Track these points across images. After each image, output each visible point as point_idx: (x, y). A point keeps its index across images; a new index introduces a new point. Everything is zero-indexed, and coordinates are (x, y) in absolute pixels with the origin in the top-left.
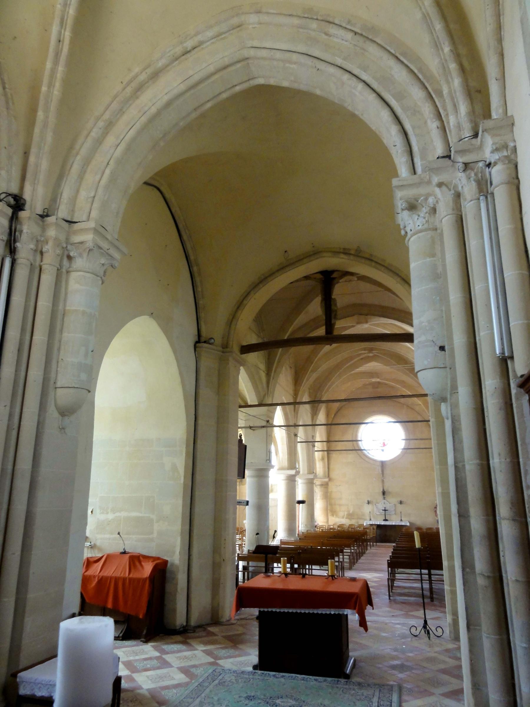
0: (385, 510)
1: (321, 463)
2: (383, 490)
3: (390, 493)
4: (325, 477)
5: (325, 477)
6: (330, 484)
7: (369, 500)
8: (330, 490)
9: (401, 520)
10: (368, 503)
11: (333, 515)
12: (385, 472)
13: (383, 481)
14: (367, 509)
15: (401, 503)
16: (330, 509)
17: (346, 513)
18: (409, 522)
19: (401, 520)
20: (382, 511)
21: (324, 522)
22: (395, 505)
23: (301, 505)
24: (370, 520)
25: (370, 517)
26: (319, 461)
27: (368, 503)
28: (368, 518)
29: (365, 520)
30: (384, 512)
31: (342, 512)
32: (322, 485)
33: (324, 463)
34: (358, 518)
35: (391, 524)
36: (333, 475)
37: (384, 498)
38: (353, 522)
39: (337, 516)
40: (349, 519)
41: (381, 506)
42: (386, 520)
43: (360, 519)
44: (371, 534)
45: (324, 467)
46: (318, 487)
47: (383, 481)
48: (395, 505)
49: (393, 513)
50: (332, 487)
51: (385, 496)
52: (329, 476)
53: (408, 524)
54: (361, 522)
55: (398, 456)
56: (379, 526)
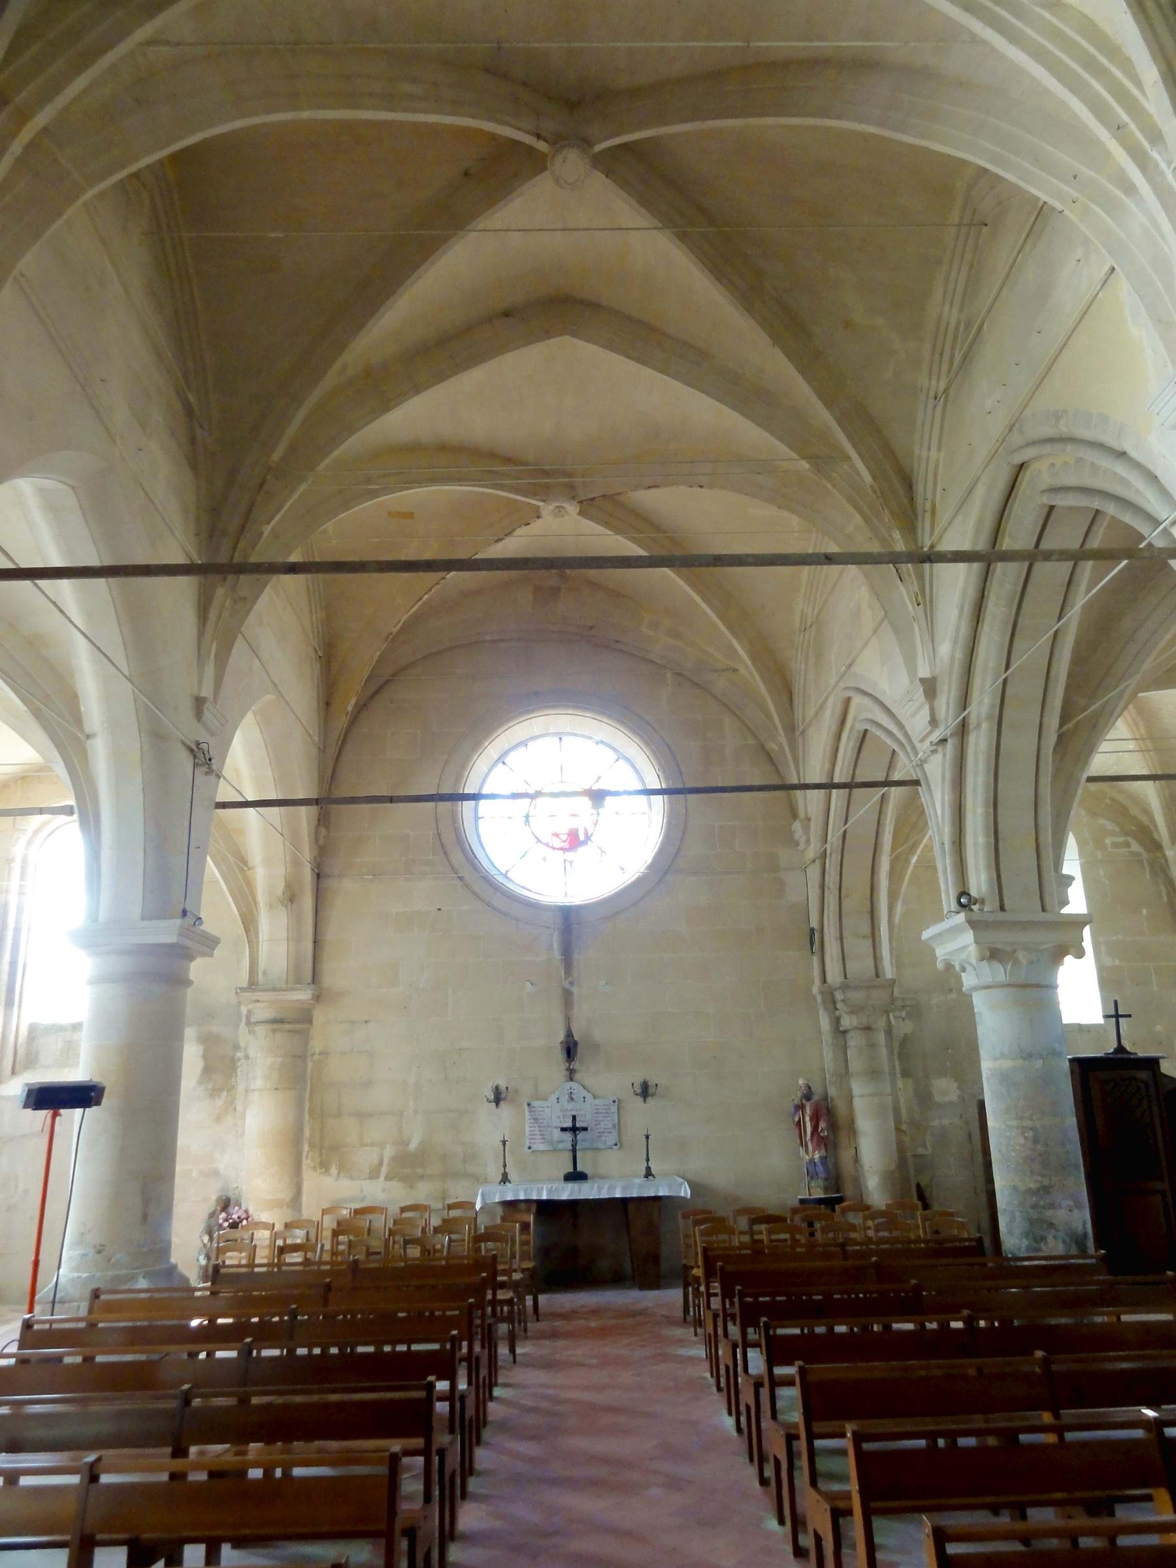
0: (574, 1129)
1: (282, 917)
2: (569, 1034)
3: (595, 1047)
4: (298, 980)
5: (298, 980)
6: (319, 1016)
7: (503, 1086)
8: (316, 1045)
9: (648, 1173)
10: (498, 1098)
11: (324, 1166)
12: (576, 956)
13: (567, 998)
14: (490, 1128)
15: (645, 1091)
16: (310, 1135)
17: (389, 1152)
18: (692, 1185)
19: (648, 1173)
20: (557, 1134)
21: (276, 1204)
22: (618, 1102)
23: (72, 1116)
24: (505, 1179)
25: (504, 1167)
27: (498, 1098)
29: (479, 1180)
30: (568, 1136)
31: (373, 1145)
32: (281, 1021)
33: (298, 918)
35: (604, 1195)
37: (571, 1074)
38: (422, 1193)
39: (345, 1169)
40: (403, 1179)
41: (556, 1114)
42: (576, 1176)
44: (518, 1257)
45: (295, 936)
46: (261, 1030)
47: (567, 998)
48: (618, 1102)
49: (612, 1139)
50: (331, 1033)
51: (576, 1065)
52: (315, 977)
53: (685, 1192)
54: (458, 1191)
56: (547, 1209)
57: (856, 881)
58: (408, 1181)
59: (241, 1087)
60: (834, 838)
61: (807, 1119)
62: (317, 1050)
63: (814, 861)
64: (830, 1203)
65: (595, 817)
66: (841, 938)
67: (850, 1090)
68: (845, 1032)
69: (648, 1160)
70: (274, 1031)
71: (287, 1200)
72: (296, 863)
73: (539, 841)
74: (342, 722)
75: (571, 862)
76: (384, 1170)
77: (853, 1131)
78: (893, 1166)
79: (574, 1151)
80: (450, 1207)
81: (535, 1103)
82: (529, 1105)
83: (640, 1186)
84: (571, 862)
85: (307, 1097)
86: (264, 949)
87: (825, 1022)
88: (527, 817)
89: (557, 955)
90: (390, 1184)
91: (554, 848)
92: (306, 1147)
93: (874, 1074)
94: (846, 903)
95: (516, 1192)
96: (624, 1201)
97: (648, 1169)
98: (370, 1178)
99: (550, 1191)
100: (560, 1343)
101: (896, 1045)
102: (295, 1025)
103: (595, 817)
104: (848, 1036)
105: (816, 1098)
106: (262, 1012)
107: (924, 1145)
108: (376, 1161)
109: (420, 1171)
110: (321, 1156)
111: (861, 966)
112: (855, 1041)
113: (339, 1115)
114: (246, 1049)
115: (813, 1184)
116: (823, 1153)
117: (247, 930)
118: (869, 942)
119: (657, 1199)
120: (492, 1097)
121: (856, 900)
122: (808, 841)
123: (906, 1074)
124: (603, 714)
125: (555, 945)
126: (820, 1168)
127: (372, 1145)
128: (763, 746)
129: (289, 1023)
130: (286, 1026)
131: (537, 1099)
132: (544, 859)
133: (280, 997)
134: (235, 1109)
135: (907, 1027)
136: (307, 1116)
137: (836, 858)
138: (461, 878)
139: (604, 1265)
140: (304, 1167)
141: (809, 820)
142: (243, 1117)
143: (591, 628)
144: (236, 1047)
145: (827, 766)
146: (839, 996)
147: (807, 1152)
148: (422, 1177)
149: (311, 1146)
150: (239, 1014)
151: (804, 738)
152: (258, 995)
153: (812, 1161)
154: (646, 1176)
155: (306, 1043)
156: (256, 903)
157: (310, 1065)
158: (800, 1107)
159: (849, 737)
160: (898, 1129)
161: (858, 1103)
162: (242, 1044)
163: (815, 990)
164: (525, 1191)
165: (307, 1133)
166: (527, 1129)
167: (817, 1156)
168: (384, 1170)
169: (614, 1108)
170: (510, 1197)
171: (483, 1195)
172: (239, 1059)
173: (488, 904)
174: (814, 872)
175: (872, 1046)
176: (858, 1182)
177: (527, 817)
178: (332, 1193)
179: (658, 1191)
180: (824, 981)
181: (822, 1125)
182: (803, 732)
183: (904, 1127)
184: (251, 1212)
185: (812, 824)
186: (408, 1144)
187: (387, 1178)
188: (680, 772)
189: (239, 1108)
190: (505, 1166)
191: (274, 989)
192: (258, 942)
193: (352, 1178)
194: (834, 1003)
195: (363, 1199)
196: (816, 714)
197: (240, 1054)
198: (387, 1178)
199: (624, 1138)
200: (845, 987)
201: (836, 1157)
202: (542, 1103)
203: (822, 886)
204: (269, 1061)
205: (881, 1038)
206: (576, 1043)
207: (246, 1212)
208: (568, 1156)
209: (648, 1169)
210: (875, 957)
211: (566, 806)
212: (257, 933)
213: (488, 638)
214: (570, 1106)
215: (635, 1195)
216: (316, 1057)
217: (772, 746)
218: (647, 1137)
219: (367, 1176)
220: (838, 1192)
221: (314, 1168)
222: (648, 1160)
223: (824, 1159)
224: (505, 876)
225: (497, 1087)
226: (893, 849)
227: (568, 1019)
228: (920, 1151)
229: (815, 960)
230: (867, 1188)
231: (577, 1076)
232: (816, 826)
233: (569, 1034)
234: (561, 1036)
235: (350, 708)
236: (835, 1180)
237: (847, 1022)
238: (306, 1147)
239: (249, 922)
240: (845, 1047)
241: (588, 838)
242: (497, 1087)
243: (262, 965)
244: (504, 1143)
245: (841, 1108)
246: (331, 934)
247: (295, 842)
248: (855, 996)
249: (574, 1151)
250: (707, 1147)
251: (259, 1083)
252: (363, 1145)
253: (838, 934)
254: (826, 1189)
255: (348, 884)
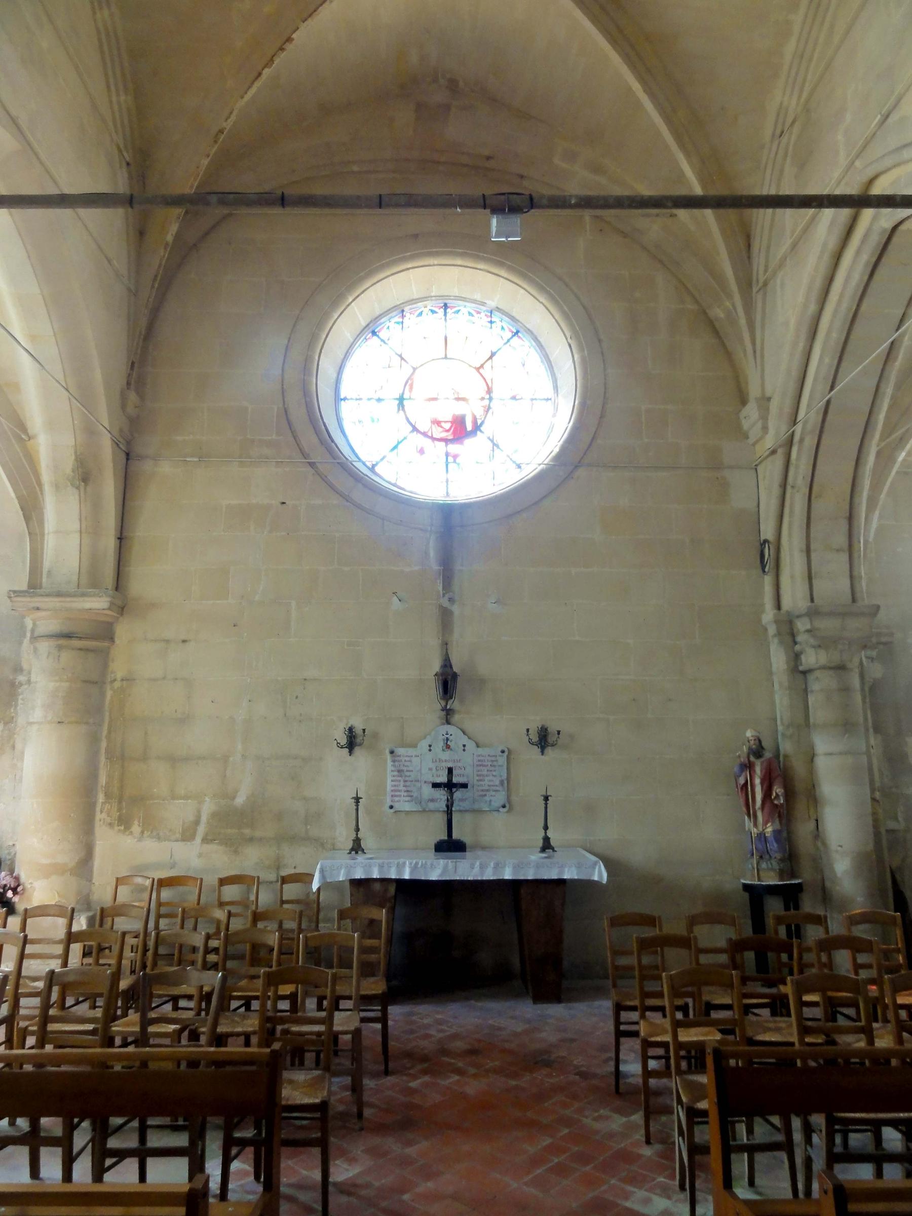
0: (450, 786)
2: (447, 664)
3: (481, 683)
6: (122, 631)
7: (359, 726)
8: (118, 668)
9: (547, 845)
10: (352, 742)
11: (124, 822)
13: (445, 619)
14: (342, 780)
15: (544, 740)
17: (208, 807)
18: (610, 864)
19: (547, 845)
20: (428, 791)
22: (508, 753)
24: (357, 847)
26: (57, 487)
27: (352, 742)
28: (344, 838)
29: (324, 845)
30: (441, 795)
31: (188, 797)
32: (68, 636)
34: (282, 838)
36: (144, 580)
37: (448, 715)
38: (251, 861)
39: (151, 827)
41: (427, 765)
42: (450, 846)
43: (293, 839)
45: (91, 527)
46: (44, 646)
47: (445, 619)
48: (508, 753)
49: (499, 798)
50: (137, 653)
51: (454, 704)
53: (600, 874)
54: (296, 859)
55: (539, 478)
56: (411, 891)
57: (835, 471)
58: (233, 845)
59: (21, 720)
60: (808, 413)
61: (757, 781)
62: (119, 675)
63: (774, 452)
64: (790, 895)
65: (486, 402)
66: (808, 551)
67: (812, 747)
68: (804, 673)
69: (546, 828)
70: (60, 648)
71: (72, 864)
72: (90, 431)
73: (415, 429)
74: (157, 258)
75: (455, 457)
76: (201, 830)
77: (814, 799)
78: (871, 847)
79: (449, 812)
80: (284, 880)
81: (400, 751)
82: (392, 752)
83: (538, 866)
84: (455, 457)
85: (105, 733)
86: (50, 542)
87: (779, 659)
88: (401, 400)
89: (436, 567)
90: (213, 847)
91: (434, 439)
92: (101, 798)
93: (847, 726)
94: (817, 505)
95: (368, 868)
96: (515, 884)
97: (546, 840)
98: (183, 840)
99: (414, 869)
100: (419, 1148)
101: (867, 689)
102: (90, 643)
103: (486, 402)
104: (811, 677)
105: (768, 755)
106: (49, 624)
107: (896, 819)
108: (191, 818)
109: (247, 831)
110: (120, 810)
111: (833, 585)
112: (820, 684)
113: (144, 758)
114: (29, 673)
115: (764, 865)
116: (777, 826)
117: (27, 519)
118: (845, 557)
119: (561, 882)
120: (344, 741)
121: (829, 504)
122: (765, 429)
123: (877, 729)
124: (500, 264)
125: (432, 553)
126: (773, 846)
127: (186, 797)
128: (705, 313)
129: (80, 638)
130: (76, 643)
131: (404, 745)
132: (422, 451)
133: (68, 605)
134: (13, 747)
135: (876, 671)
136: (103, 758)
137: (810, 442)
138: (312, 465)
139: (485, 958)
140: (97, 824)
141: (769, 399)
142: (21, 758)
143: (488, 158)
144: (18, 669)
145: (813, 308)
146: (802, 625)
147: (755, 825)
148: (251, 840)
149: (108, 796)
150: (23, 627)
151: (765, 294)
152: (37, 601)
153: (762, 836)
154: (543, 850)
155: (105, 665)
156: (40, 484)
157: (109, 693)
158: (748, 766)
159: (858, 252)
160: (874, 800)
161: (821, 763)
162: (25, 666)
163: (768, 615)
164: (381, 867)
165: (103, 780)
166: (389, 784)
167: (769, 829)
168: (201, 830)
169: (502, 760)
170: (359, 875)
171: (322, 871)
172: (21, 684)
173: (347, 498)
174: (772, 470)
175: (845, 689)
176: (819, 863)
177: (401, 400)
178: (132, 858)
179: (562, 872)
180: (778, 606)
181: (778, 790)
182: (765, 284)
183: (877, 795)
184: (23, 878)
185: (774, 406)
186: (234, 798)
187: (205, 840)
188: (600, 341)
189: (19, 746)
190: (357, 830)
191: (59, 594)
192: (43, 535)
193: (159, 838)
194: (793, 635)
195: (173, 866)
196: (794, 246)
197: (22, 678)
198: (205, 840)
199: (514, 798)
200: (813, 613)
201: (789, 833)
202: (411, 751)
203: (784, 486)
204: (52, 685)
205: (856, 682)
206: (455, 676)
207: (17, 879)
208: (442, 819)
209: (546, 840)
210: (852, 577)
211: (452, 383)
212: (41, 522)
213: (355, 168)
214: (446, 755)
215: (530, 878)
216: (117, 685)
217: (718, 313)
218: (546, 798)
219: (178, 836)
220: (793, 875)
221: (111, 825)
222: (546, 828)
223: (776, 833)
224: (372, 469)
225: (351, 730)
226: (882, 439)
227: (445, 645)
228: (892, 825)
229: (768, 580)
230: (832, 870)
231: (456, 718)
232: (779, 405)
233: (447, 664)
234: (436, 667)
235: (170, 238)
236: (790, 859)
237: (810, 659)
238: (101, 798)
239: (31, 509)
240: (806, 691)
241: (477, 428)
242: (351, 730)
243: (46, 565)
244: (357, 800)
245: (799, 768)
246: (141, 531)
247: (82, 396)
248: (827, 625)
249: (449, 812)
250: (610, 809)
251: (38, 714)
252: (174, 797)
253: (804, 547)
254: (782, 874)
255: (165, 468)
